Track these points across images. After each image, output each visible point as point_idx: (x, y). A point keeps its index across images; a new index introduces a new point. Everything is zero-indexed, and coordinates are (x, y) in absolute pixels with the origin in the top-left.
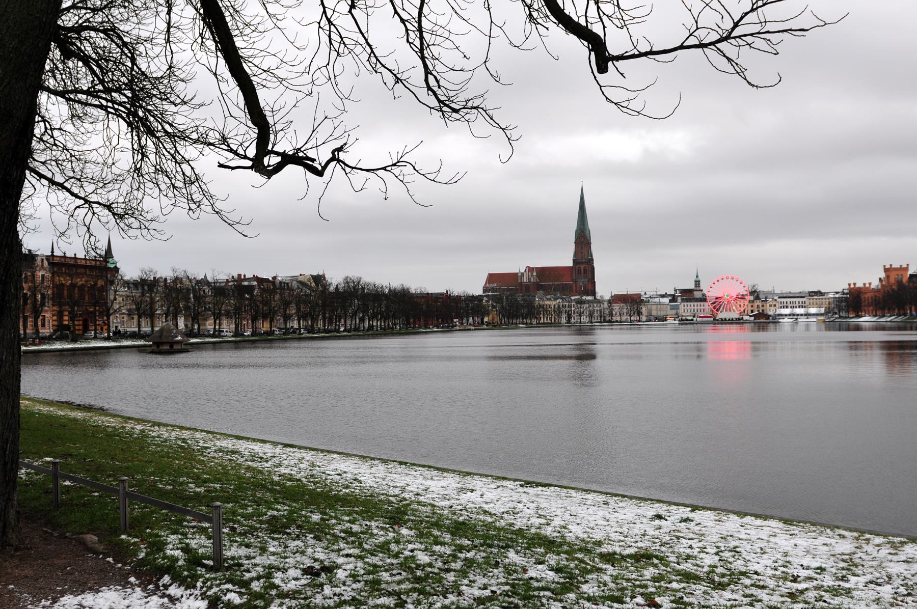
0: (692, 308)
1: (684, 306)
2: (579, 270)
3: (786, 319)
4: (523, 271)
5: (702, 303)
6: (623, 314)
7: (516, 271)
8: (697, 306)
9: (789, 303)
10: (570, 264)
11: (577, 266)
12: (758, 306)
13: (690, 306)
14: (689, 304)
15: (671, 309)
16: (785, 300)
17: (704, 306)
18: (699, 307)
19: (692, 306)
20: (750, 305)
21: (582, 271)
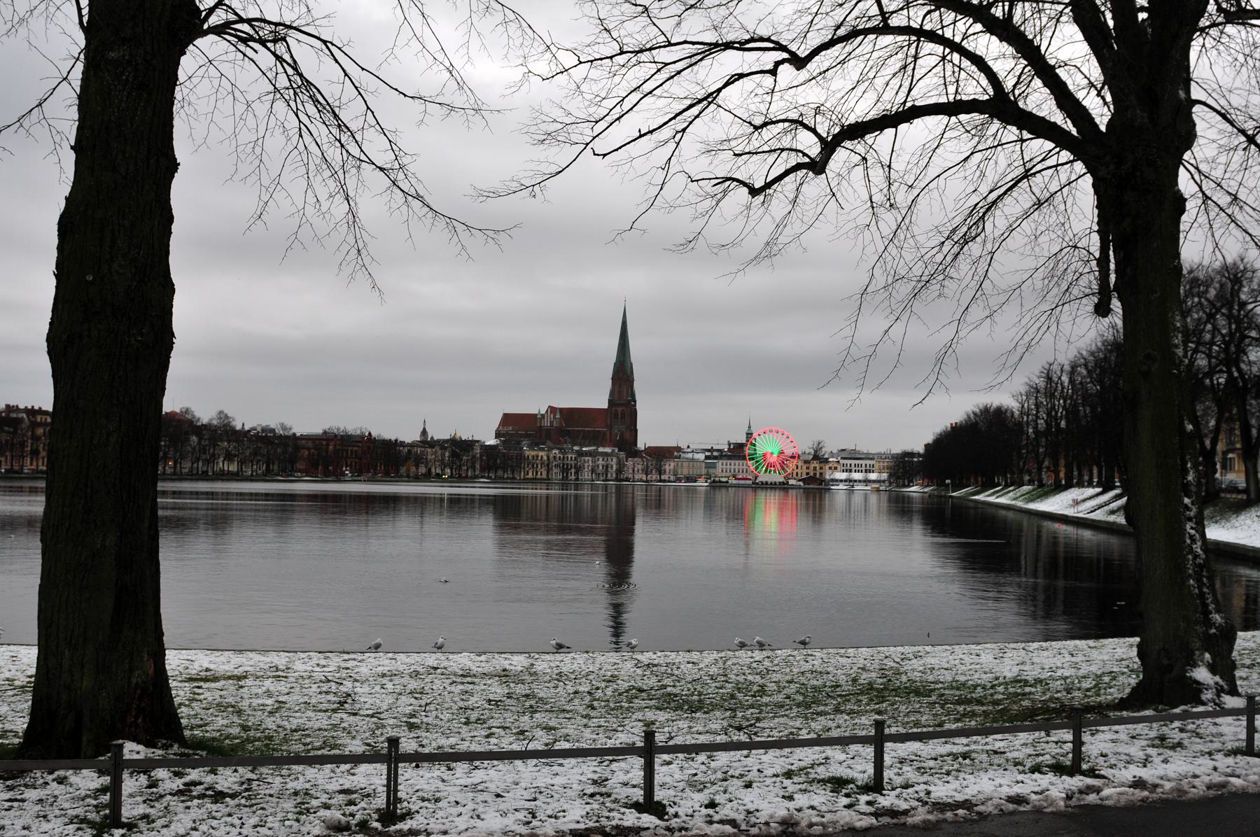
1: (722, 464)
2: (616, 414)
3: (841, 486)
4: (543, 412)
6: (638, 471)
7: (536, 412)
9: (853, 465)
10: (605, 405)
11: (614, 409)
12: (815, 468)
15: (706, 468)
16: (849, 462)
20: (804, 467)
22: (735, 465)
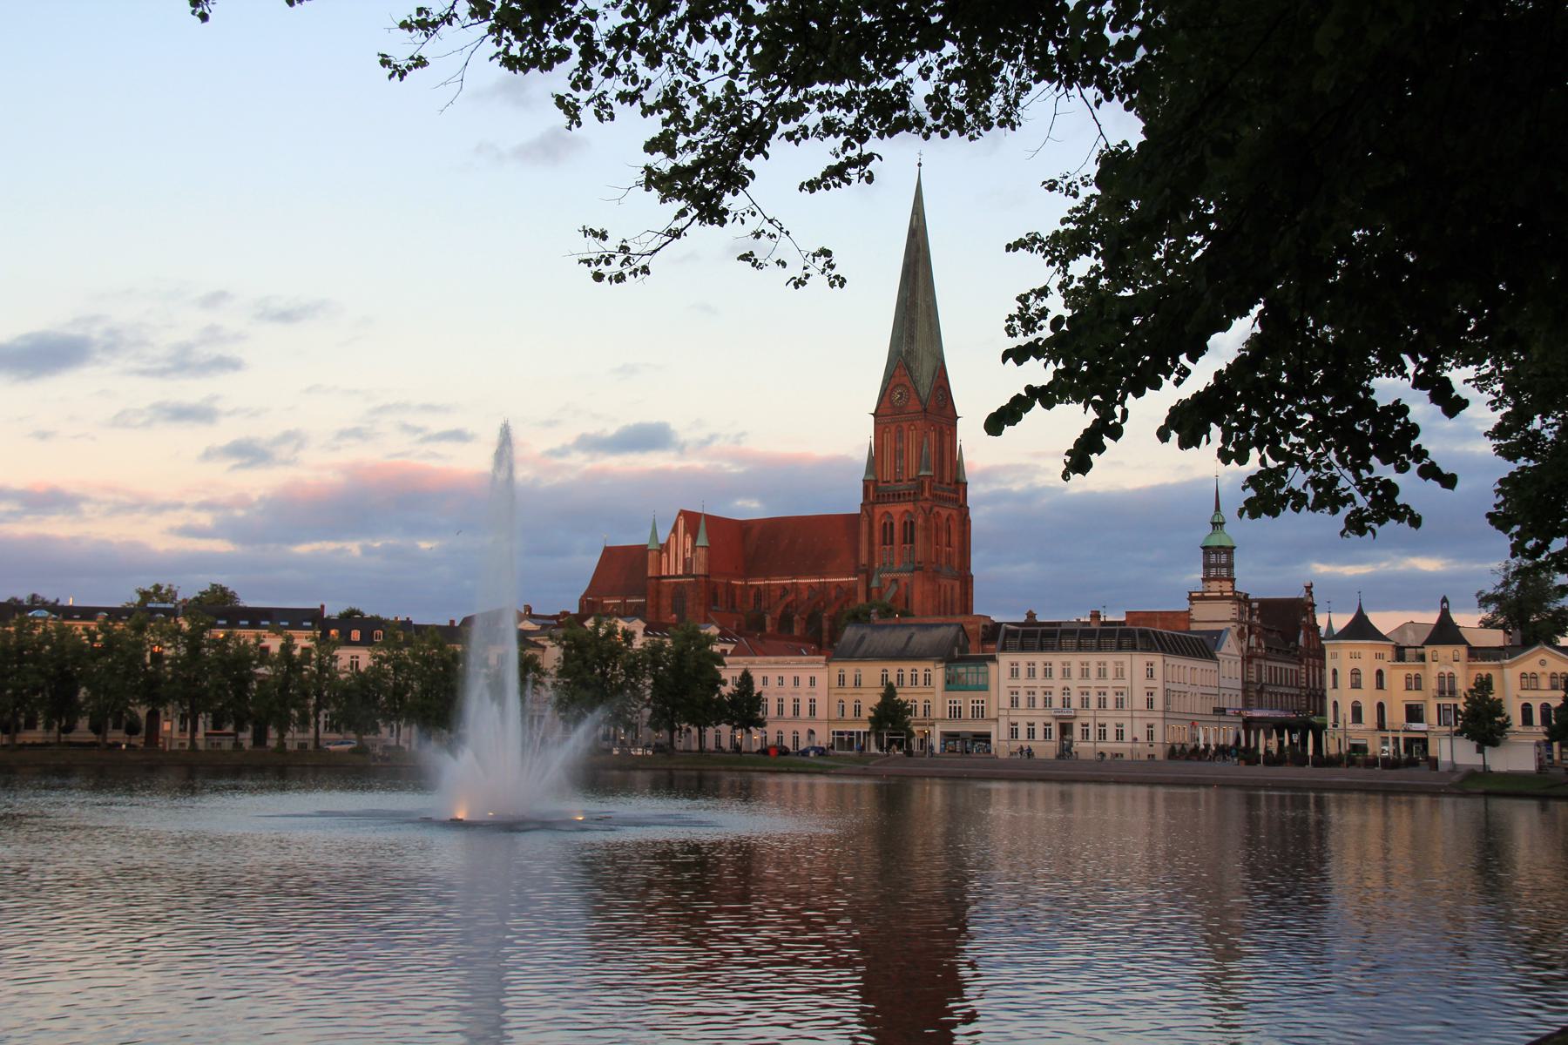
1: (1014, 673)
2: (888, 529)
4: (663, 535)
11: (879, 510)
13: (1048, 673)
17: (1119, 674)
18: (1093, 682)
20: (1396, 677)
21: (897, 526)
22: (1066, 674)
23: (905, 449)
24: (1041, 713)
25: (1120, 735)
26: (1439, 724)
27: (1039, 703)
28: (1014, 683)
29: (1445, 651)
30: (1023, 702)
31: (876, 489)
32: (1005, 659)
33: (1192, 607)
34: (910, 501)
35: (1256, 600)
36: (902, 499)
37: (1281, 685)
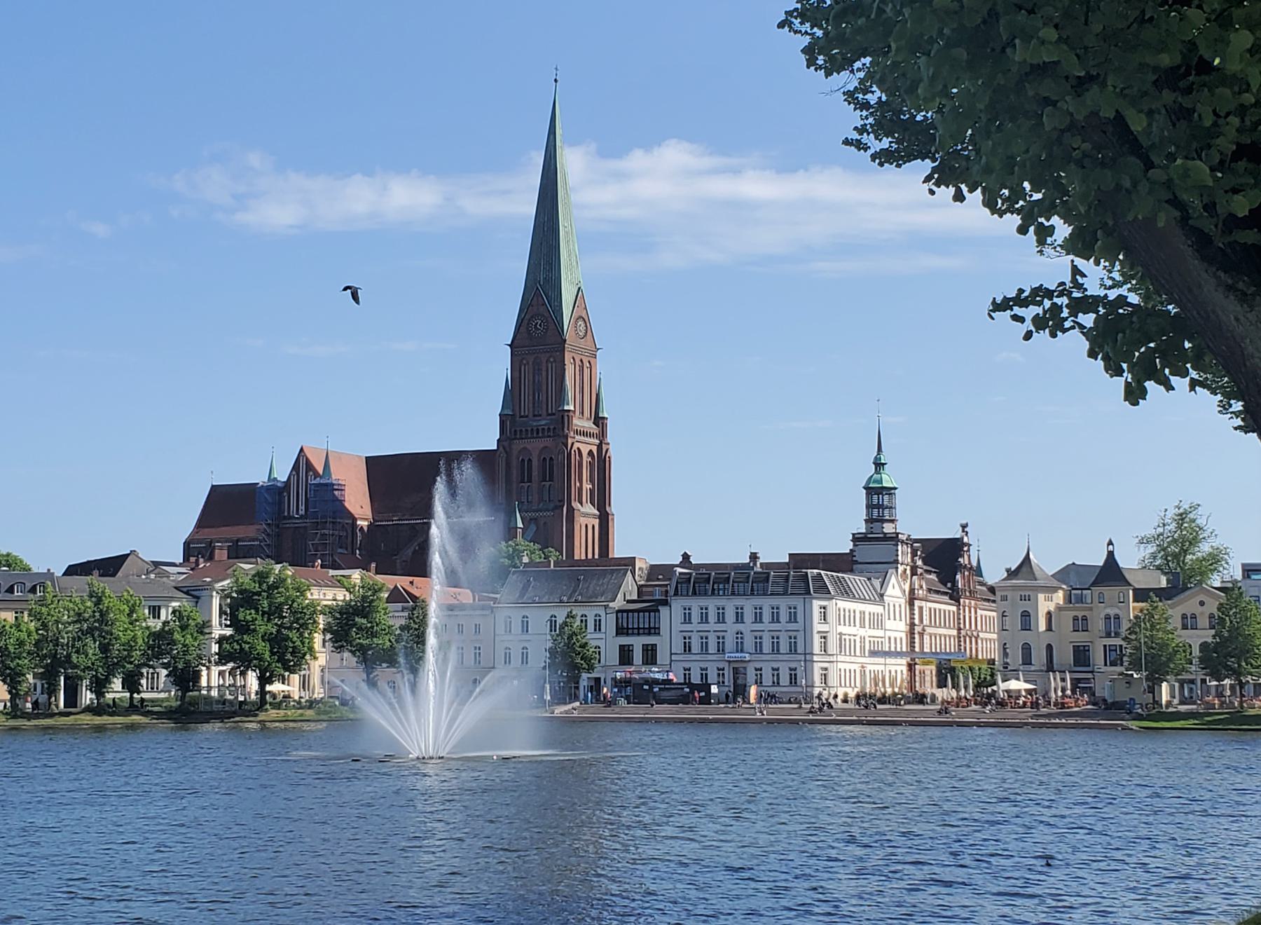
0: (731, 627)
1: (687, 619)
2: (526, 465)
5: (783, 603)
8: (758, 618)
11: (518, 445)
14: (712, 604)
19: (730, 615)
23: (544, 381)
24: (768, 658)
25: (793, 680)
26: (1106, 665)
27: (712, 648)
28: (687, 627)
29: (1110, 592)
30: (696, 647)
31: (513, 423)
32: (678, 605)
33: (856, 548)
34: (549, 436)
35: (917, 541)
36: (540, 435)
37: (940, 627)
